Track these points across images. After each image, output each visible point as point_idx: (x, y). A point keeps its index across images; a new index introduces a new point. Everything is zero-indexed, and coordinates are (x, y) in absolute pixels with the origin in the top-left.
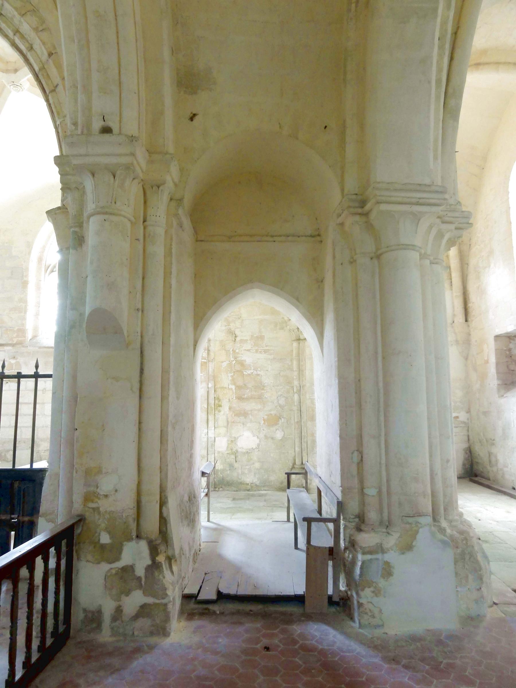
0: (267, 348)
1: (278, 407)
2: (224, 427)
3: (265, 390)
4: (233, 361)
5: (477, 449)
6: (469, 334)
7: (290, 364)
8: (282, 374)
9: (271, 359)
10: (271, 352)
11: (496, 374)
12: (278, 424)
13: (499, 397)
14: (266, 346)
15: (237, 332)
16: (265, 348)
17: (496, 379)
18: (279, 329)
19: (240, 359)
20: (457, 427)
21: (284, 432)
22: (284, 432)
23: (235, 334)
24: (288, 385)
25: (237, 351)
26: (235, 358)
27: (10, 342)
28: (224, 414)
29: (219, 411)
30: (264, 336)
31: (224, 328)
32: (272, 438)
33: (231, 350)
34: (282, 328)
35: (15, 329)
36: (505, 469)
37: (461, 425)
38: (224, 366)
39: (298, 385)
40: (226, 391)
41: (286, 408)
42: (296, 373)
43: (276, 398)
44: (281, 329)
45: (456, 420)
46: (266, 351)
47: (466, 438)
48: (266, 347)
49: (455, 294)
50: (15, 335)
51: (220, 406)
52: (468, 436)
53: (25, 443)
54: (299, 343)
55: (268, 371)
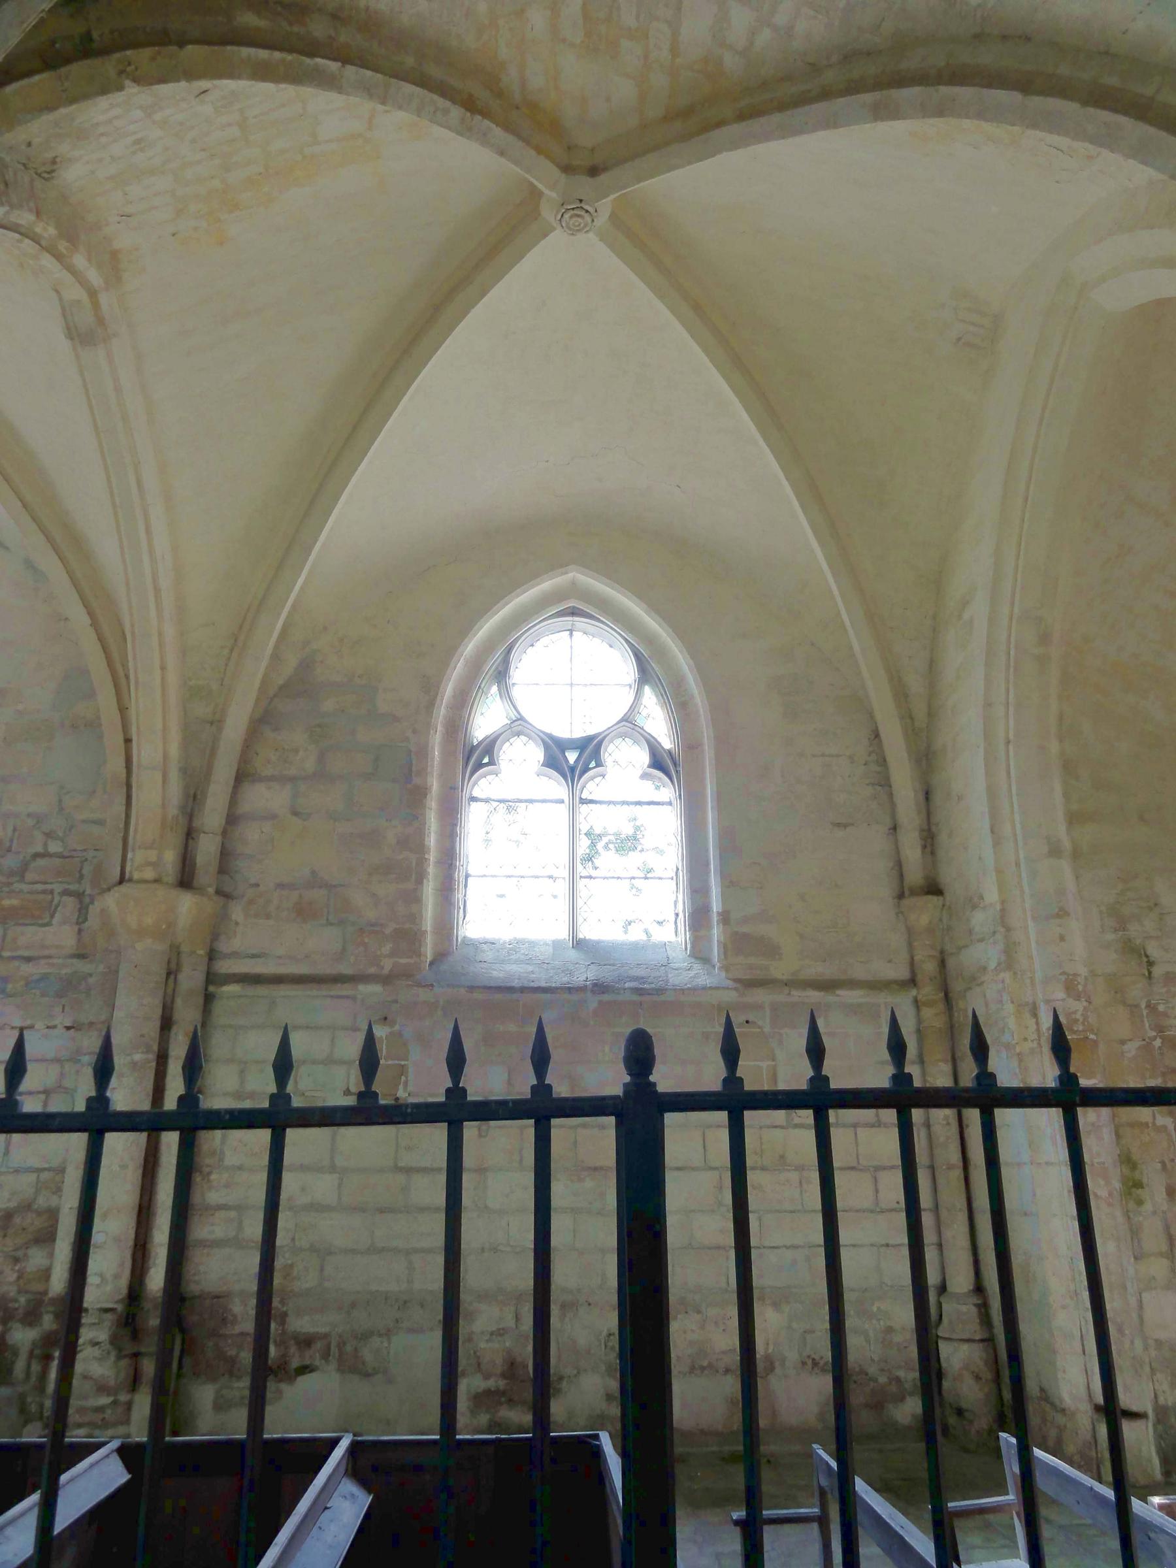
2: (1161, 1254)
4: (1155, 1038)
15: (1153, 950)
19: (1172, 1033)
23: (1147, 956)
25: (1161, 1008)
26: (1160, 1029)
27: (372, 970)
28: (1154, 1213)
29: (1140, 1202)
31: (1110, 936)
33: (1143, 1005)
35: (388, 931)
38: (1129, 1055)
40: (1149, 1134)
50: (387, 948)
51: (1138, 1185)
53: (422, 1306)
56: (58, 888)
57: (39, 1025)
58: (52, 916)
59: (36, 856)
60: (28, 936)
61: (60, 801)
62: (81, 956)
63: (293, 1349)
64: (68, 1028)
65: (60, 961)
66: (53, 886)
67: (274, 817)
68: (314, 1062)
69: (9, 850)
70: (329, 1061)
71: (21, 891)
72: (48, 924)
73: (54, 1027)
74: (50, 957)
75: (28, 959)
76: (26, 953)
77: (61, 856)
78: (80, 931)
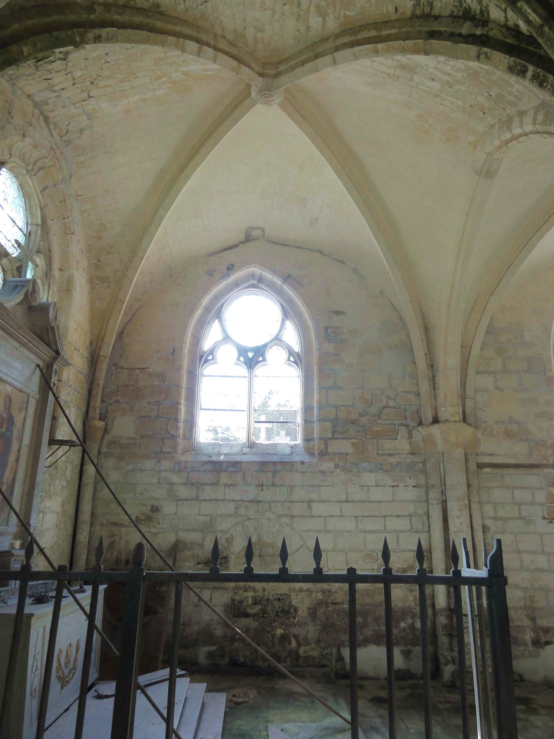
27: (545, 462)
35: (549, 444)
50: (549, 452)
56: (397, 422)
57: (401, 485)
58: (397, 435)
59: (384, 407)
60: (388, 445)
61: (390, 382)
62: (413, 454)
63: (541, 633)
64: (414, 487)
65: (405, 456)
66: (394, 422)
67: (486, 390)
68: (527, 504)
69: (372, 404)
70: (533, 504)
71: (381, 424)
72: (396, 439)
73: (408, 486)
74: (399, 454)
75: (390, 455)
76: (389, 452)
77: (394, 407)
78: (410, 442)
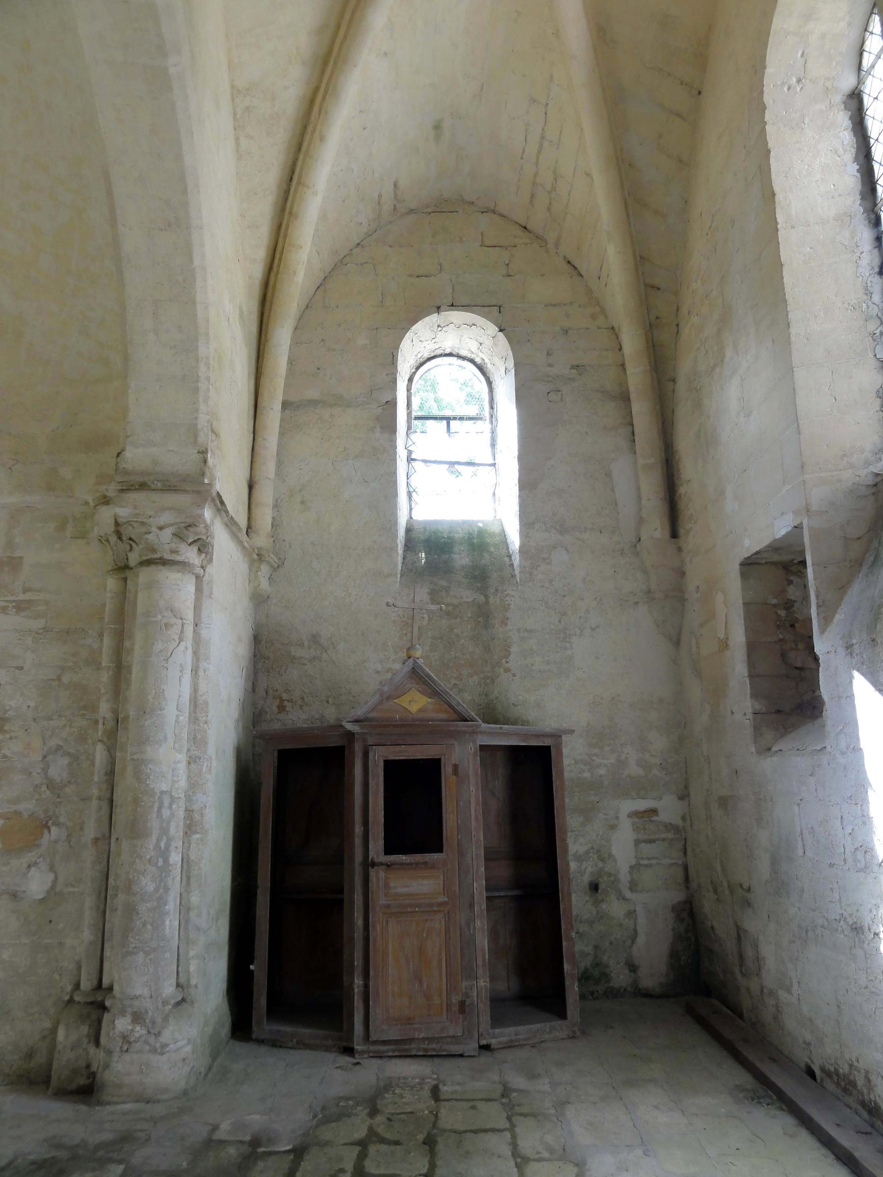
0: (28, 596)
1: (44, 788)
3: (6, 731)
5: (707, 905)
6: (682, 573)
7: (96, 646)
8: (65, 679)
9: (37, 633)
10: (40, 608)
11: (747, 681)
12: (39, 846)
13: (759, 753)
14: (25, 590)
16: (21, 597)
17: (749, 696)
18: (72, 538)
20: (654, 841)
21: (56, 873)
22: (56, 873)
24: (83, 714)
30: (21, 558)
32: (15, 896)
34: (82, 535)
36: (782, 995)
37: (663, 836)
39: (109, 716)
41: (68, 790)
42: (105, 677)
43: (40, 759)
44: (76, 538)
45: (651, 821)
46: (20, 607)
47: (679, 873)
48: (24, 593)
49: (641, 461)
52: (686, 868)
54: (125, 580)
55: (21, 668)
